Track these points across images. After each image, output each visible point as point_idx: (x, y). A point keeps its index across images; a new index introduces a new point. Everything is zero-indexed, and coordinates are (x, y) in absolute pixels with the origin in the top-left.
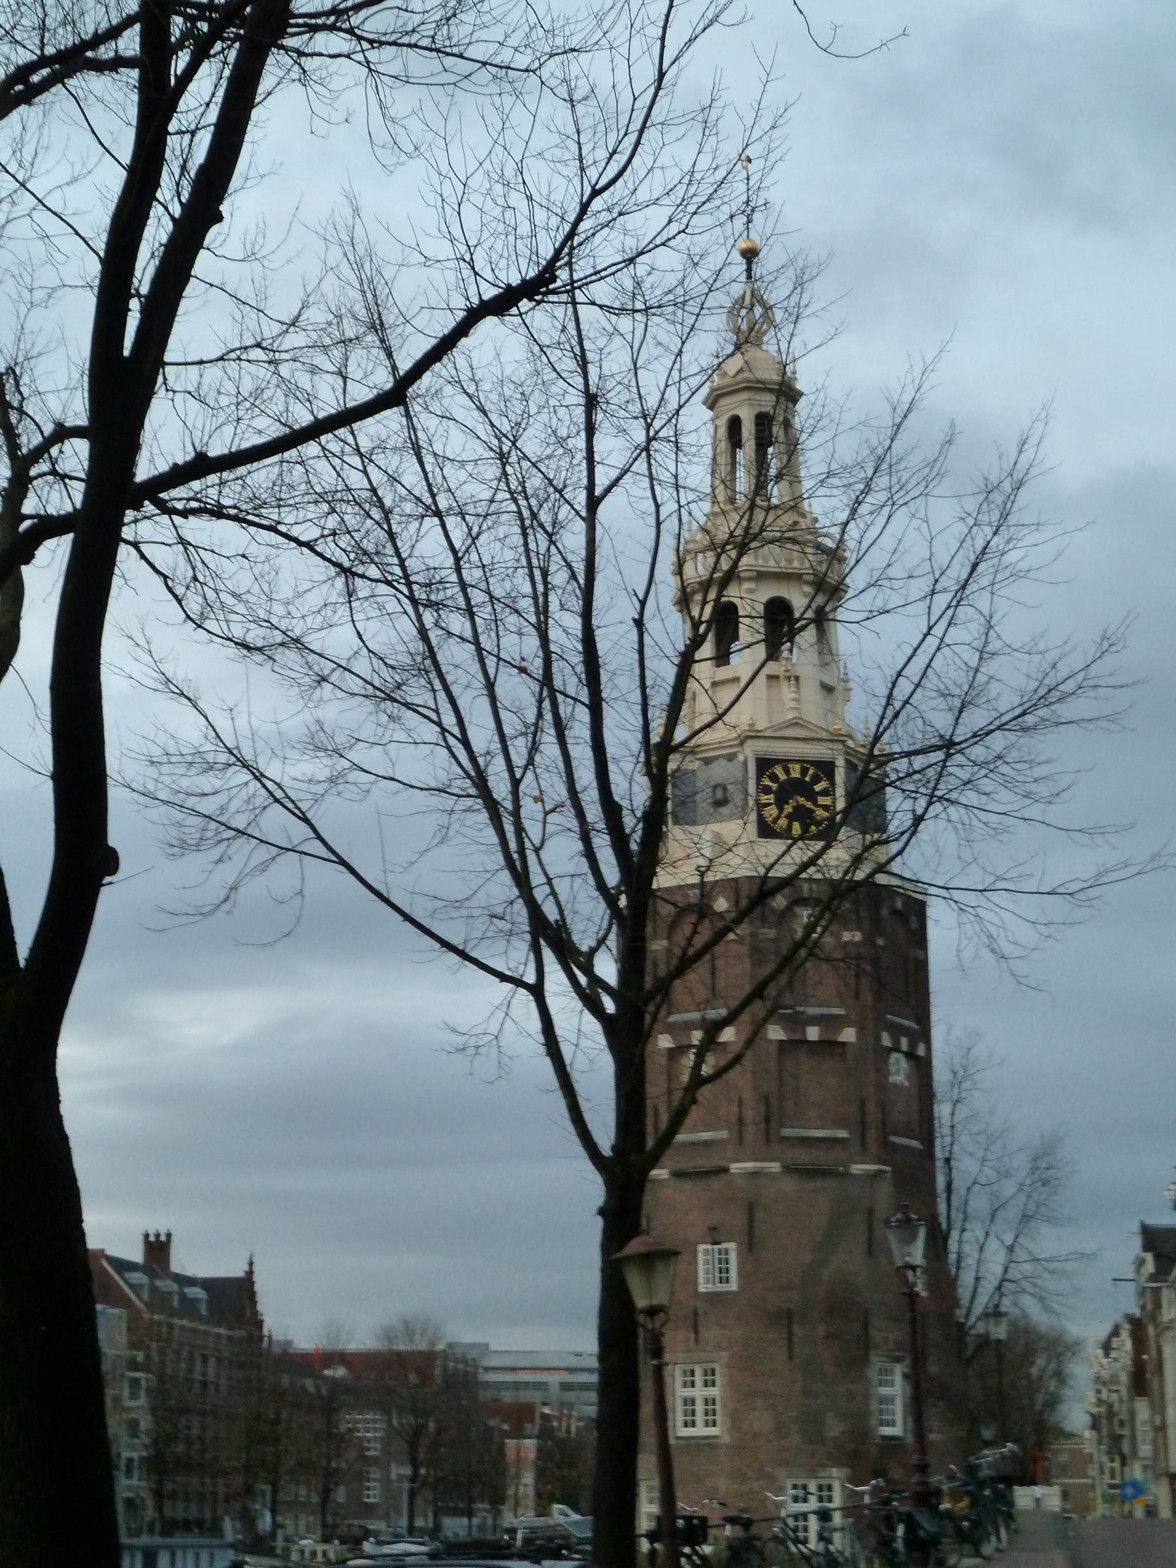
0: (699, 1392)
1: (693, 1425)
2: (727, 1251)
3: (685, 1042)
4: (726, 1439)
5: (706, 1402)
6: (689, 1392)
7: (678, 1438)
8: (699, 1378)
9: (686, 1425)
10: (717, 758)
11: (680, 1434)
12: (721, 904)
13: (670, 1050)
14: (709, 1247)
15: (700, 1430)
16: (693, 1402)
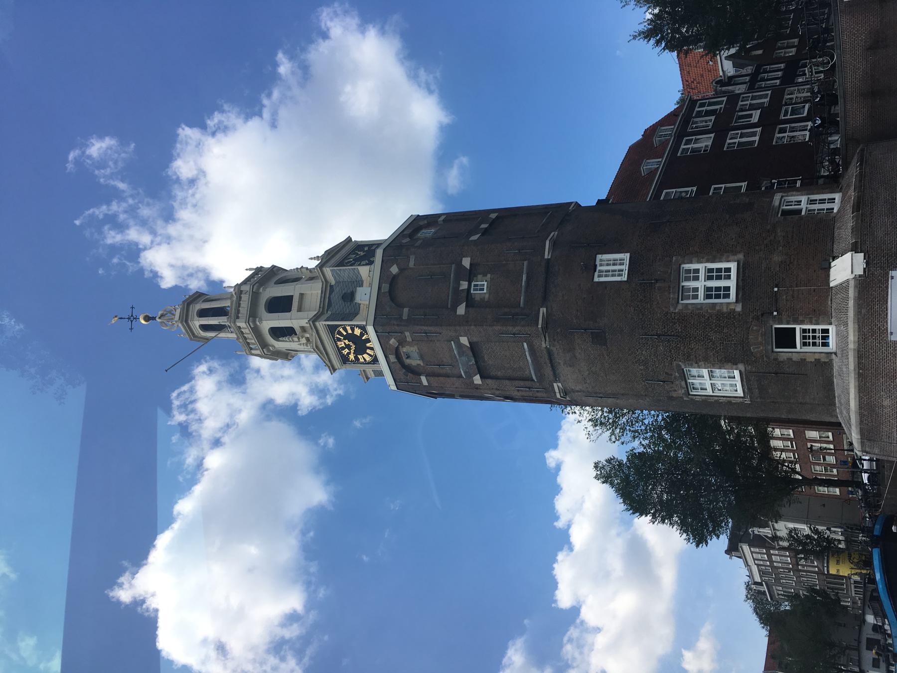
0: (701, 284)
1: (727, 289)
2: (601, 260)
3: (464, 295)
4: (741, 256)
5: (710, 278)
6: (701, 294)
7: (737, 301)
8: (692, 284)
9: (727, 296)
10: (329, 298)
11: (734, 300)
12: (394, 270)
13: (467, 306)
14: (596, 274)
15: (732, 283)
16: (708, 289)
